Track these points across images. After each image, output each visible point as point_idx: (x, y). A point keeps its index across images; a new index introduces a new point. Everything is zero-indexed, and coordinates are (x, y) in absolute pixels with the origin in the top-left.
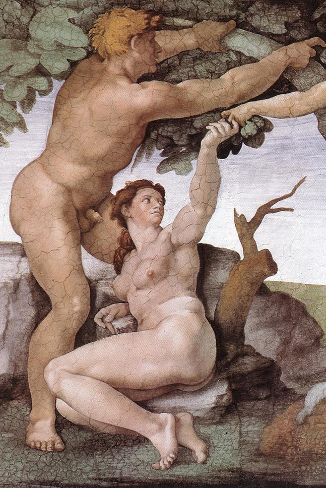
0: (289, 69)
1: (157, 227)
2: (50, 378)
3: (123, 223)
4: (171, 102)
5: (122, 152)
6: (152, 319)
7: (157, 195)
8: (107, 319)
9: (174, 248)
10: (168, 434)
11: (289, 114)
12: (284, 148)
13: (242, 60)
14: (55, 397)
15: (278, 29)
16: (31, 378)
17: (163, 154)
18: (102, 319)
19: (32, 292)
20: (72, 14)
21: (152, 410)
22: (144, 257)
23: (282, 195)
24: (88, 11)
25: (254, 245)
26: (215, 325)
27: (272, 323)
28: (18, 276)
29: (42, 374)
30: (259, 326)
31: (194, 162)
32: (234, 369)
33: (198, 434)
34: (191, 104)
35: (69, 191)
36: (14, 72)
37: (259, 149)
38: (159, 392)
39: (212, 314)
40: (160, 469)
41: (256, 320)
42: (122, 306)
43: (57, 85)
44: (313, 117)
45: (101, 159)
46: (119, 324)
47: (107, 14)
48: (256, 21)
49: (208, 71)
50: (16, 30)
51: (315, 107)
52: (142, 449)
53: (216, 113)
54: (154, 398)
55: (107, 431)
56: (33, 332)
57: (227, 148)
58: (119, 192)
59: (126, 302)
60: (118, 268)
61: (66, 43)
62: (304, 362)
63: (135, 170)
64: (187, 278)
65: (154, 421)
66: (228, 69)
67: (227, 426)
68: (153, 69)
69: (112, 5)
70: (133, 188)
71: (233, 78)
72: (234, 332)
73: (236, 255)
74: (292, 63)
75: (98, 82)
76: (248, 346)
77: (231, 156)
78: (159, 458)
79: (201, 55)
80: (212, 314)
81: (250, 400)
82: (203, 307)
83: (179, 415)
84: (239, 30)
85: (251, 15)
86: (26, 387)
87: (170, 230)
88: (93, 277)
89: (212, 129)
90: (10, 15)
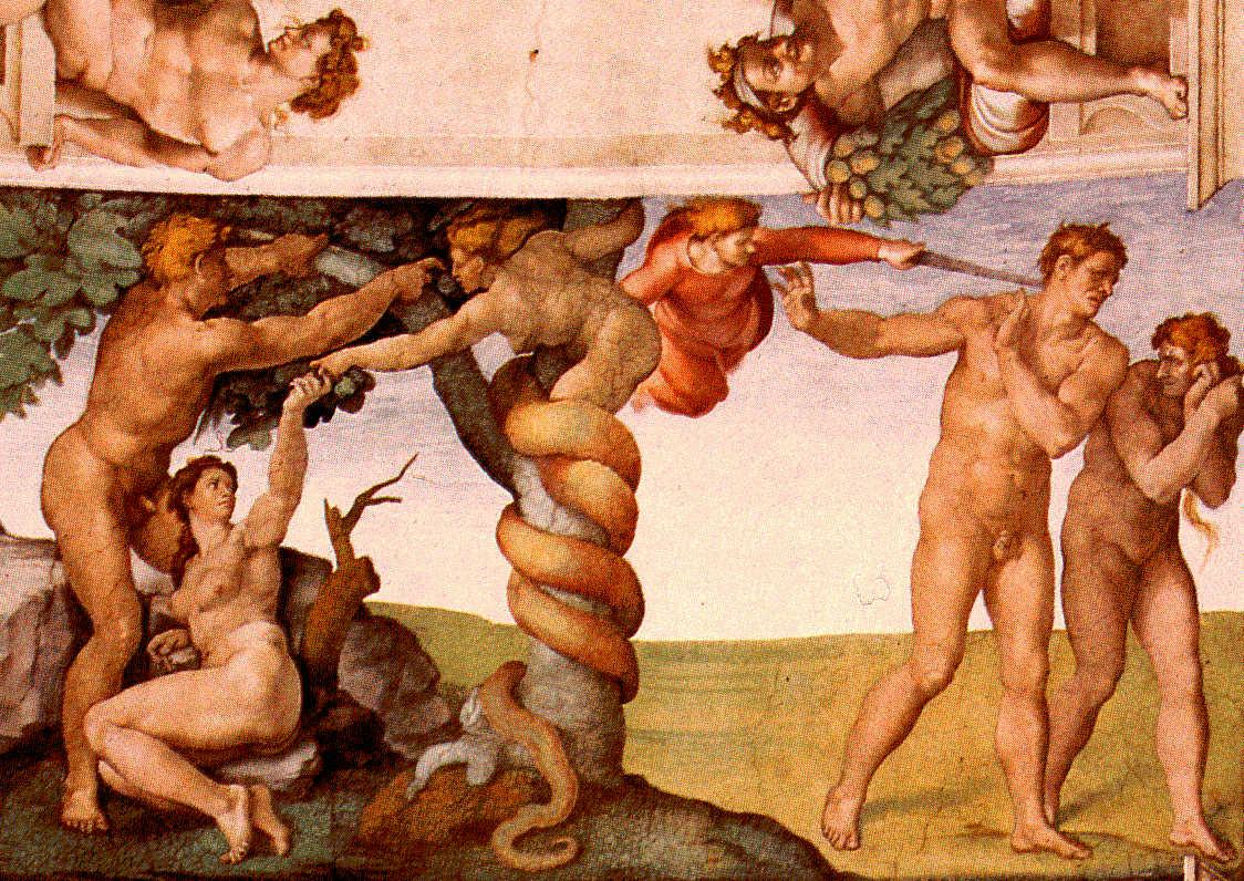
1: (227, 524)
4: (246, 348)
9: (250, 553)
10: (240, 809)
12: (387, 414)
19: (69, 610)
25: (350, 550)
31: (274, 432)
33: (276, 811)
35: (115, 469)
39: (297, 644)
44: (427, 370)
53: (302, 365)
56: (70, 665)
57: (317, 412)
73: (326, 564)
74: (400, 294)
77: (321, 424)
80: (297, 644)
86: (61, 741)
89: (298, 388)
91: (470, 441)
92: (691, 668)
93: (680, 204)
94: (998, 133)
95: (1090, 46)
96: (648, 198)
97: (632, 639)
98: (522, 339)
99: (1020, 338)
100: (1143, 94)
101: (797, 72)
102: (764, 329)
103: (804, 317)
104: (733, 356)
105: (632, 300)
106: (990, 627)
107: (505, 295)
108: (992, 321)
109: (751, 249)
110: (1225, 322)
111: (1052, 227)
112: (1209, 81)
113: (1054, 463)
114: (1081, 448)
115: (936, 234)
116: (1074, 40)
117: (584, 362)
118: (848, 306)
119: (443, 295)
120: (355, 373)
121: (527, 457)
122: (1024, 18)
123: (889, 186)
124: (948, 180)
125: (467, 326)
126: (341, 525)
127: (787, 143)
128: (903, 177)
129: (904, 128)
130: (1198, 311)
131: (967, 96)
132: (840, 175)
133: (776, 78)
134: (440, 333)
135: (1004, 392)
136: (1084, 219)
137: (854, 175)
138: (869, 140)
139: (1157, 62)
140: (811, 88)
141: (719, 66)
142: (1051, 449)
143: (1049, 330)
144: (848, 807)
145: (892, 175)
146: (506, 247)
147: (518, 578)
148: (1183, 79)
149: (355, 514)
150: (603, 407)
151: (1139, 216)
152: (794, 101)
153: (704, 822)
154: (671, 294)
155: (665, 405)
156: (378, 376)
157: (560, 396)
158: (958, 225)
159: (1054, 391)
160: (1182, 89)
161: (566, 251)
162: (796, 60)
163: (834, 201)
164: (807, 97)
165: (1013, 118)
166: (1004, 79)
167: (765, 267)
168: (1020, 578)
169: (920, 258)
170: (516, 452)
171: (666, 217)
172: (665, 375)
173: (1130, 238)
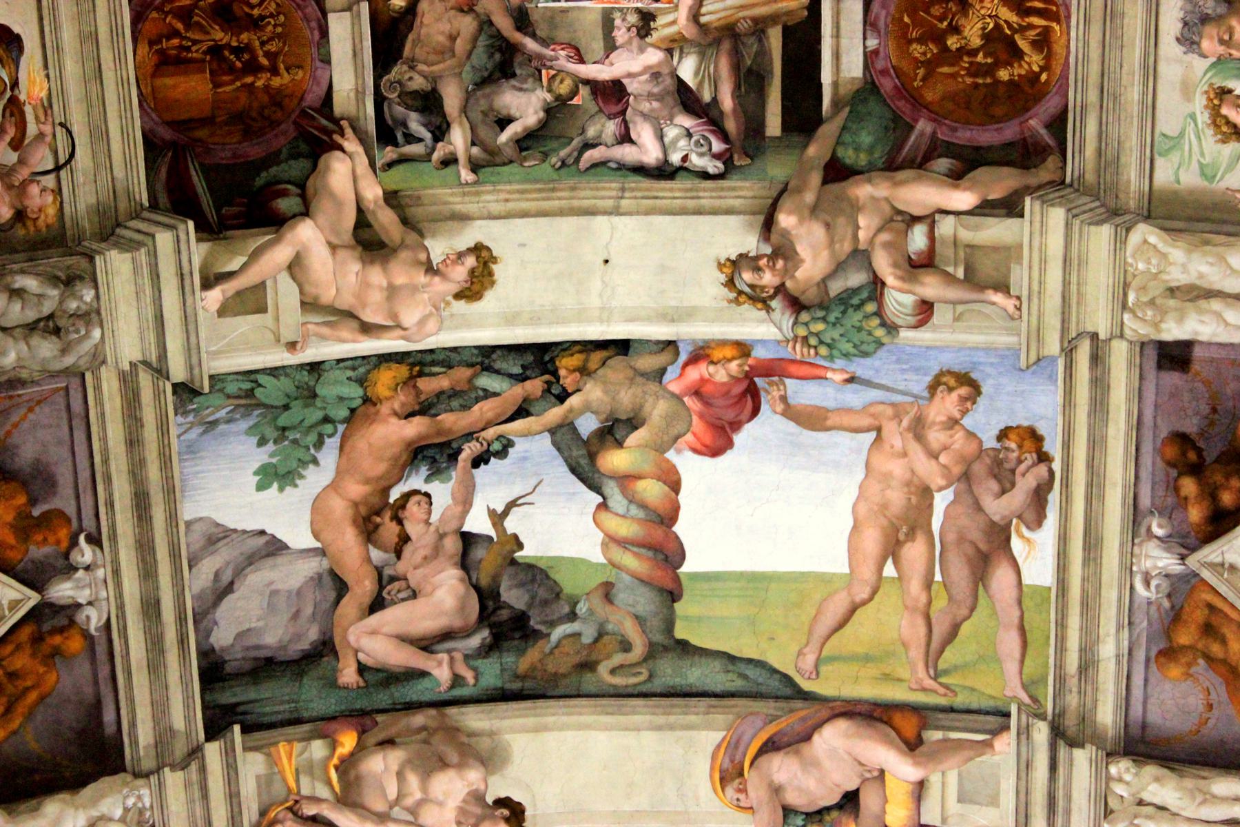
0: (525, 400)
1: (427, 523)
2: (352, 638)
3: (400, 522)
5: (396, 471)
6: (429, 588)
7: (427, 500)
8: (393, 593)
9: (442, 536)
11: (527, 434)
12: (525, 459)
13: (488, 394)
14: (356, 651)
15: (517, 370)
16: (337, 641)
17: (428, 470)
18: (389, 593)
20: (349, 373)
21: (432, 652)
22: (418, 545)
23: (524, 493)
24: (362, 370)
25: (504, 530)
26: (477, 588)
27: (521, 585)
28: (321, 571)
29: (345, 638)
30: (510, 588)
32: (494, 619)
33: (468, 665)
34: (450, 431)
36: (307, 423)
37: (505, 461)
38: (436, 640)
39: (474, 580)
40: (440, 692)
41: (509, 583)
42: (403, 583)
43: (341, 428)
44: (547, 434)
45: (380, 478)
46: (401, 596)
47: (376, 371)
48: (497, 365)
49: (461, 405)
50: (305, 393)
51: (549, 427)
52: (426, 680)
53: (469, 436)
54: (432, 644)
55: (397, 670)
57: (479, 461)
58: (395, 501)
59: (406, 579)
60: (398, 554)
61: (346, 396)
62: (548, 611)
63: (408, 483)
64: (451, 557)
65: (434, 660)
66: (477, 402)
67: (491, 660)
68: (417, 408)
69: (381, 363)
70: (407, 496)
71: (481, 409)
72: (492, 592)
73: (490, 538)
75: (373, 422)
76: (504, 602)
77: (483, 466)
78: (439, 685)
79: (454, 394)
81: (506, 640)
82: (466, 577)
83: (454, 654)
84: (484, 373)
85: (494, 361)
87: (437, 524)
88: (380, 565)
90: (299, 381)
91: (573, 470)
92: (715, 585)
93: (701, 344)
94: (902, 316)
95: (960, 273)
96: (683, 341)
97: (678, 571)
98: (605, 416)
99: (916, 426)
100: (994, 304)
101: (774, 275)
102: (756, 411)
103: (780, 407)
104: (736, 426)
105: (673, 395)
106: (896, 575)
107: (593, 392)
108: (897, 417)
109: (747, 368)
110: (1042, 429)
111: (935, 370)
112: (1035, 300)
113: (936, 495)
114: (952, 489)
115: (861, 367)
116: (950, 269)
117: (645, 427)
118: (808, 403)
119: (554, 395)
120: (502, 439)
121: (611, 477)
122: (919, 254)
123: (833, 340)
124: (870, 339)
125: (571, 410)
126: (498, 518)
127: (768, 312)
128: (841, 335)
129: (842, 308)
130: (1026, 423)
131: (882, 294)
132: (802, 332)
133: (761, 278)
134: (555, 414)
135: (905, 454)
136: (956, 368)
137: (811, 333)
138: (820, 314)
139: (1003, 287)
140: (783, 284)
141: (725, 270)
142: (933, 487)
143: (934, 423)
144: (810, 659)
145: (835, 334)
146: (592, 365)
147: (607, 540)
148: (1019, 298)
149: (506, 512)
150: (656, 450)
151: (988, 370)
152: (772, 291)
153: (725, 661)
154: (696, 392)
155: (696, 451)
156: (515, 439)
157: (630, 445)
158: (877, 363)
159: (936, 458)
160: (1017, 303)
161: (631, 367)
162: (773, 268)
163: (798, 347)
164: (780, 289)
165: (910, 308)
166: (906, 286)
167: (756, 379)
168: (914, 552)
169: (851, 380)
170: (603, 475)
171: (694, 351)
172: (694, 434)
173: (984, 380)
